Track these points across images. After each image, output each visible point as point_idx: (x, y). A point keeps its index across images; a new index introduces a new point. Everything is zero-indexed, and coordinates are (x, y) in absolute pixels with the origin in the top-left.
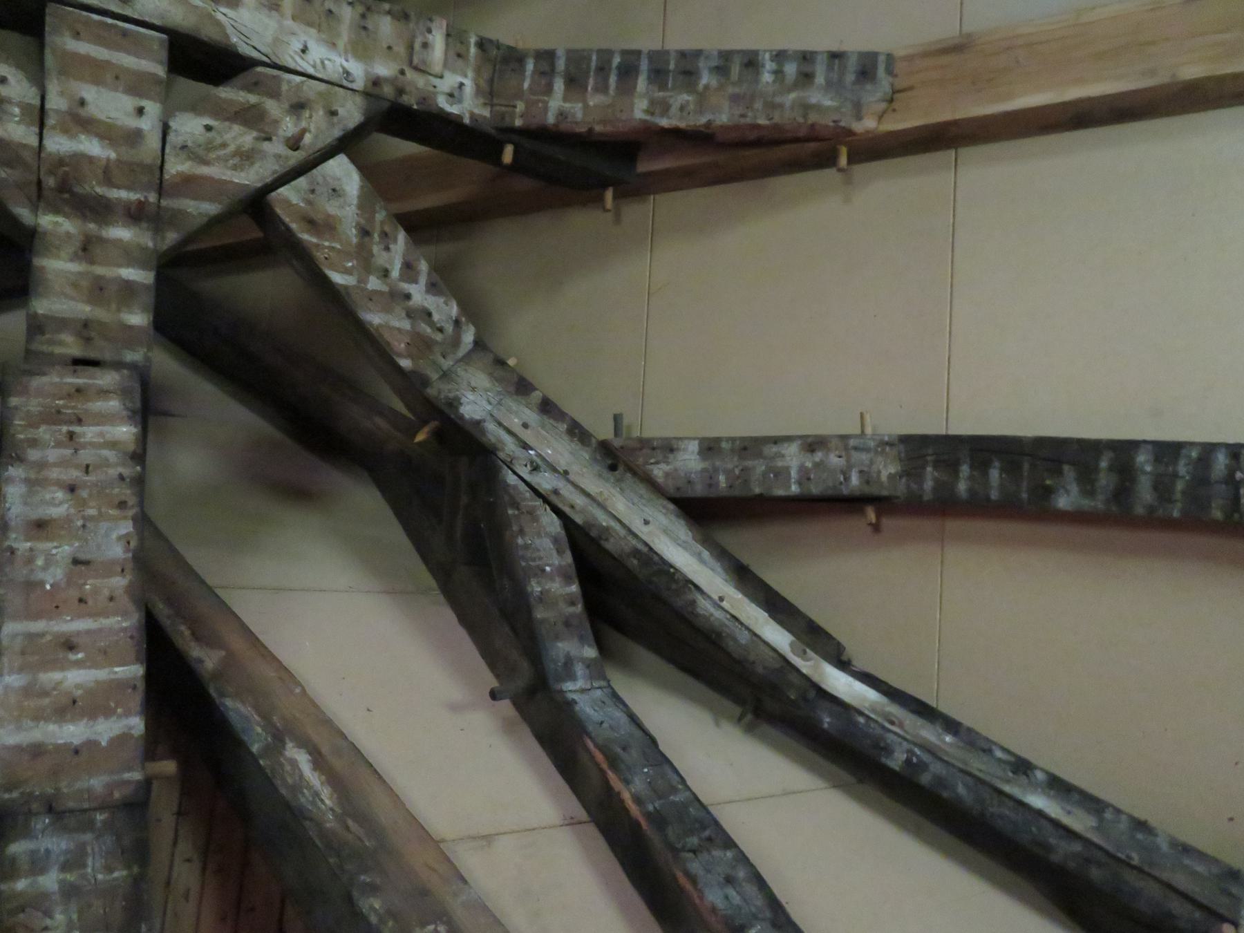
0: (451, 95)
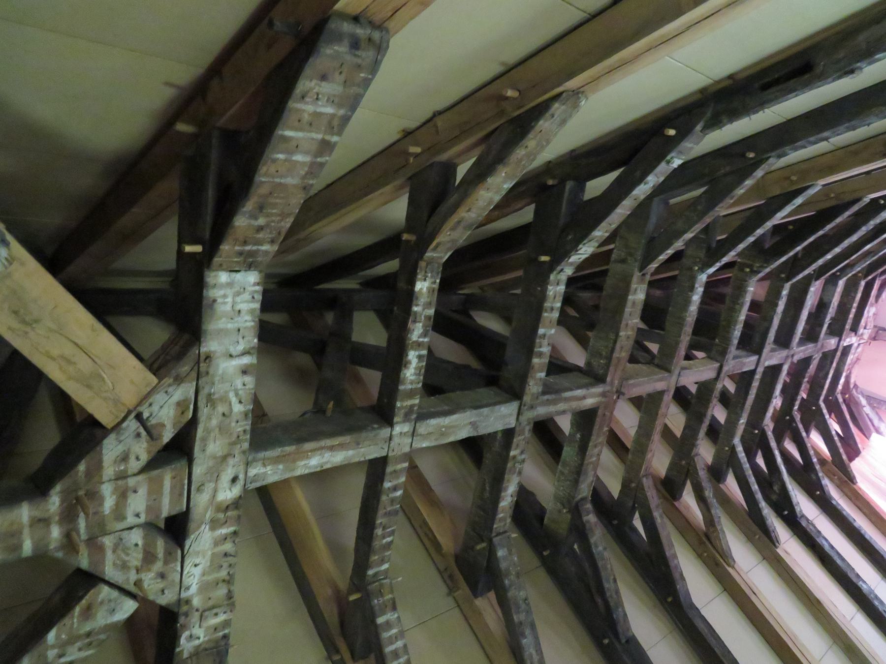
0: (191, 636)
